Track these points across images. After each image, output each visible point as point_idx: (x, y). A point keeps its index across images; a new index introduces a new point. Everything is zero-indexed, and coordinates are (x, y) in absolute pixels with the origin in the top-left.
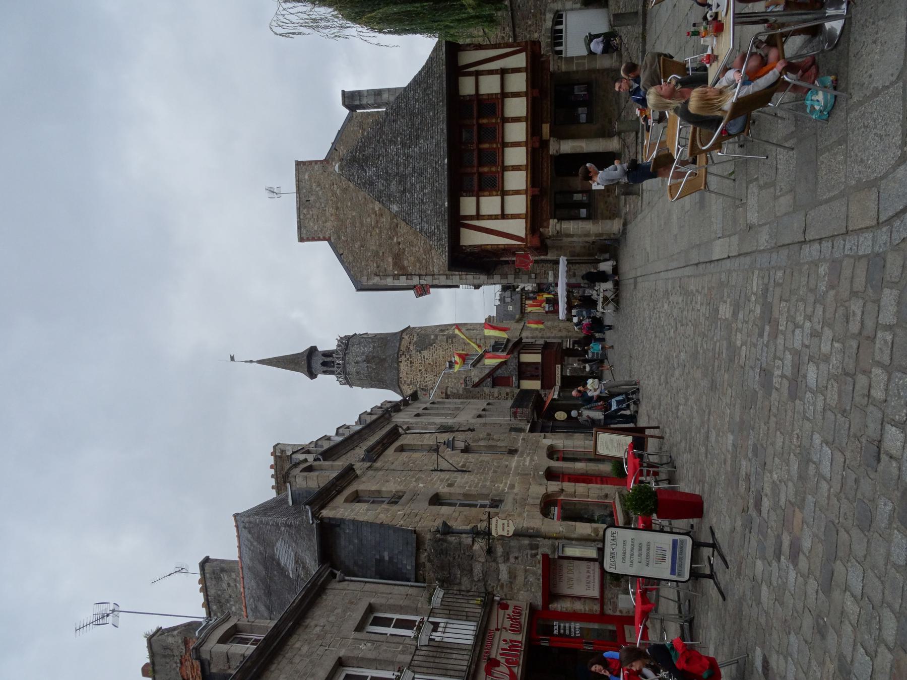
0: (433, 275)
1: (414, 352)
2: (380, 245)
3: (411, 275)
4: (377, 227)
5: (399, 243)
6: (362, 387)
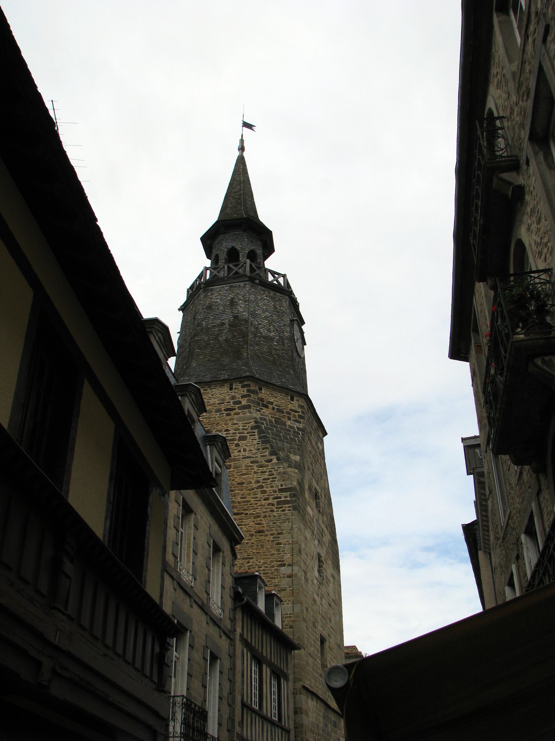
1: (258, 415)
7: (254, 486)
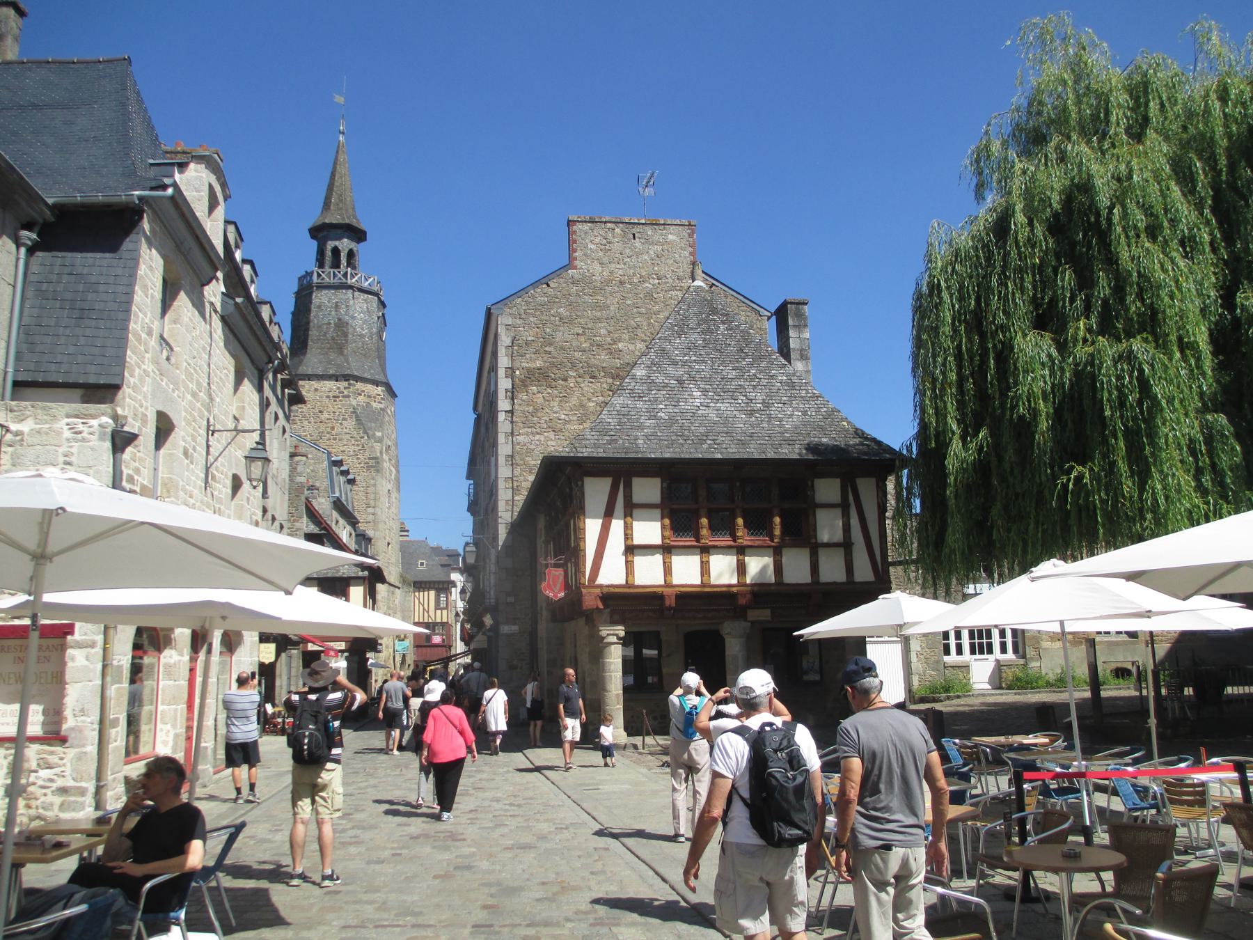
0: (512, 433)
1: (354, 402)
2: (562, 348)
3: (513, 399)
4: (592, 345)
5: (565, 380)
6: (294, 314)
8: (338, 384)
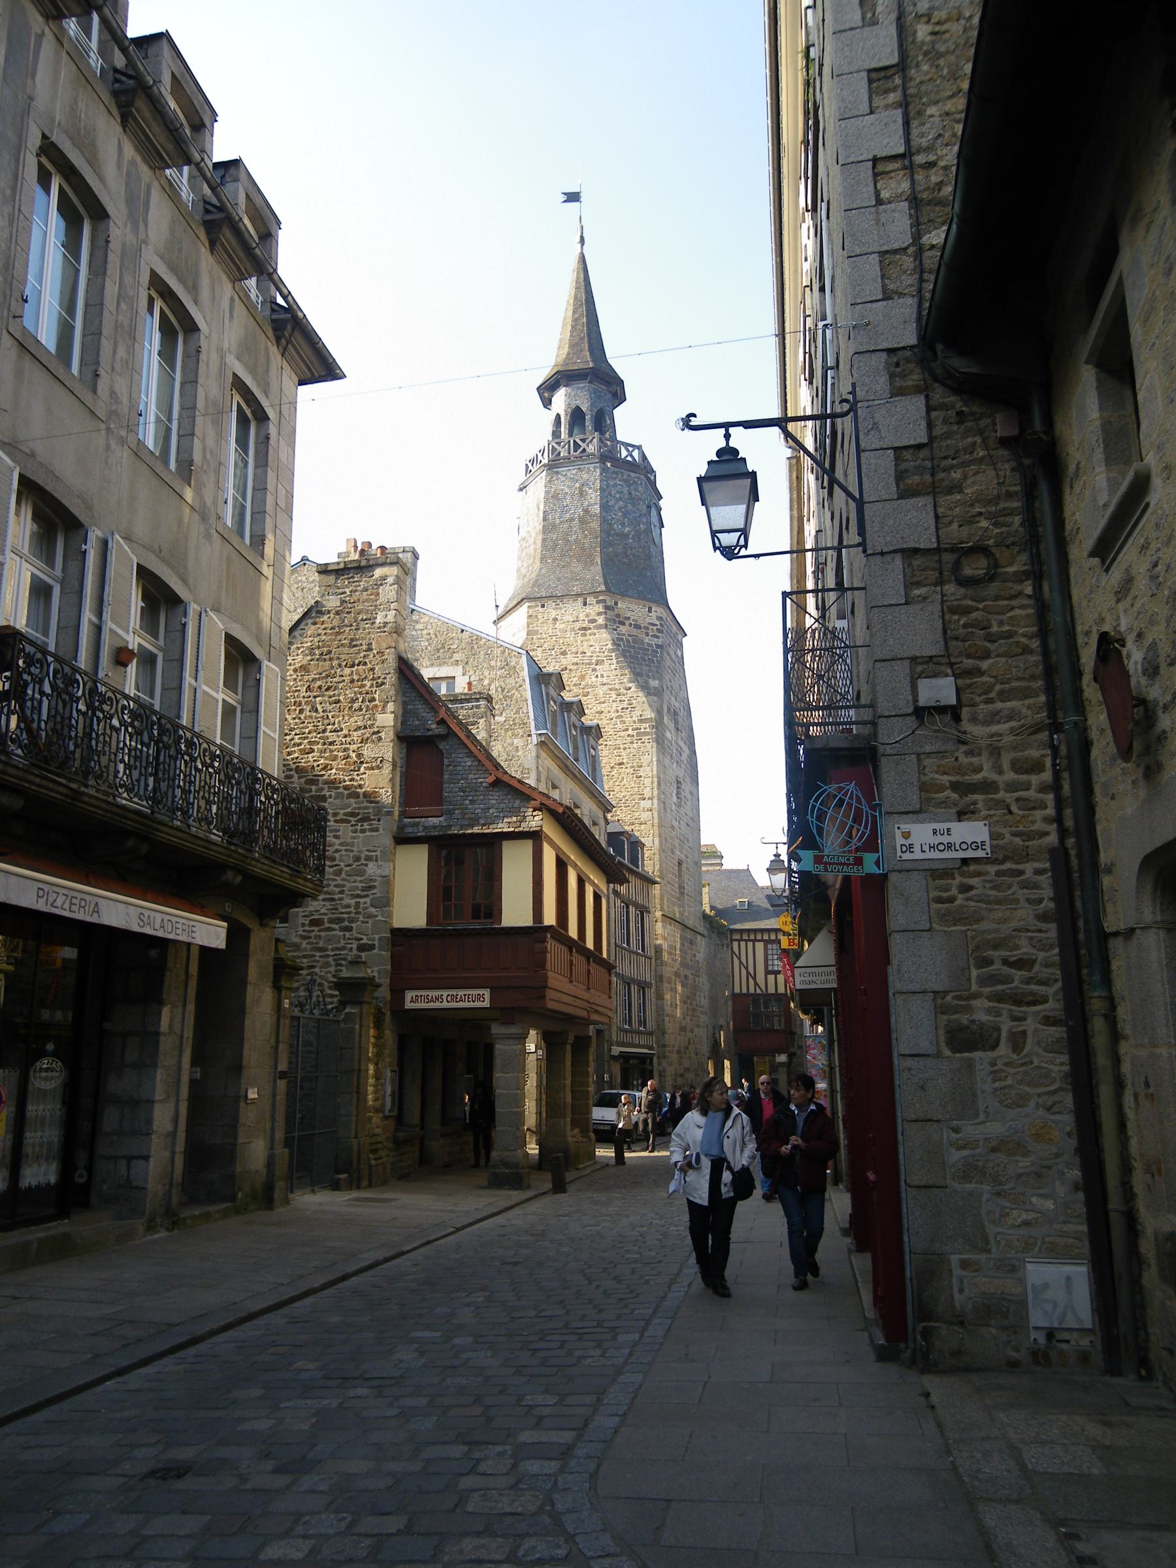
7: (614, 715)
8: (588, 609)
